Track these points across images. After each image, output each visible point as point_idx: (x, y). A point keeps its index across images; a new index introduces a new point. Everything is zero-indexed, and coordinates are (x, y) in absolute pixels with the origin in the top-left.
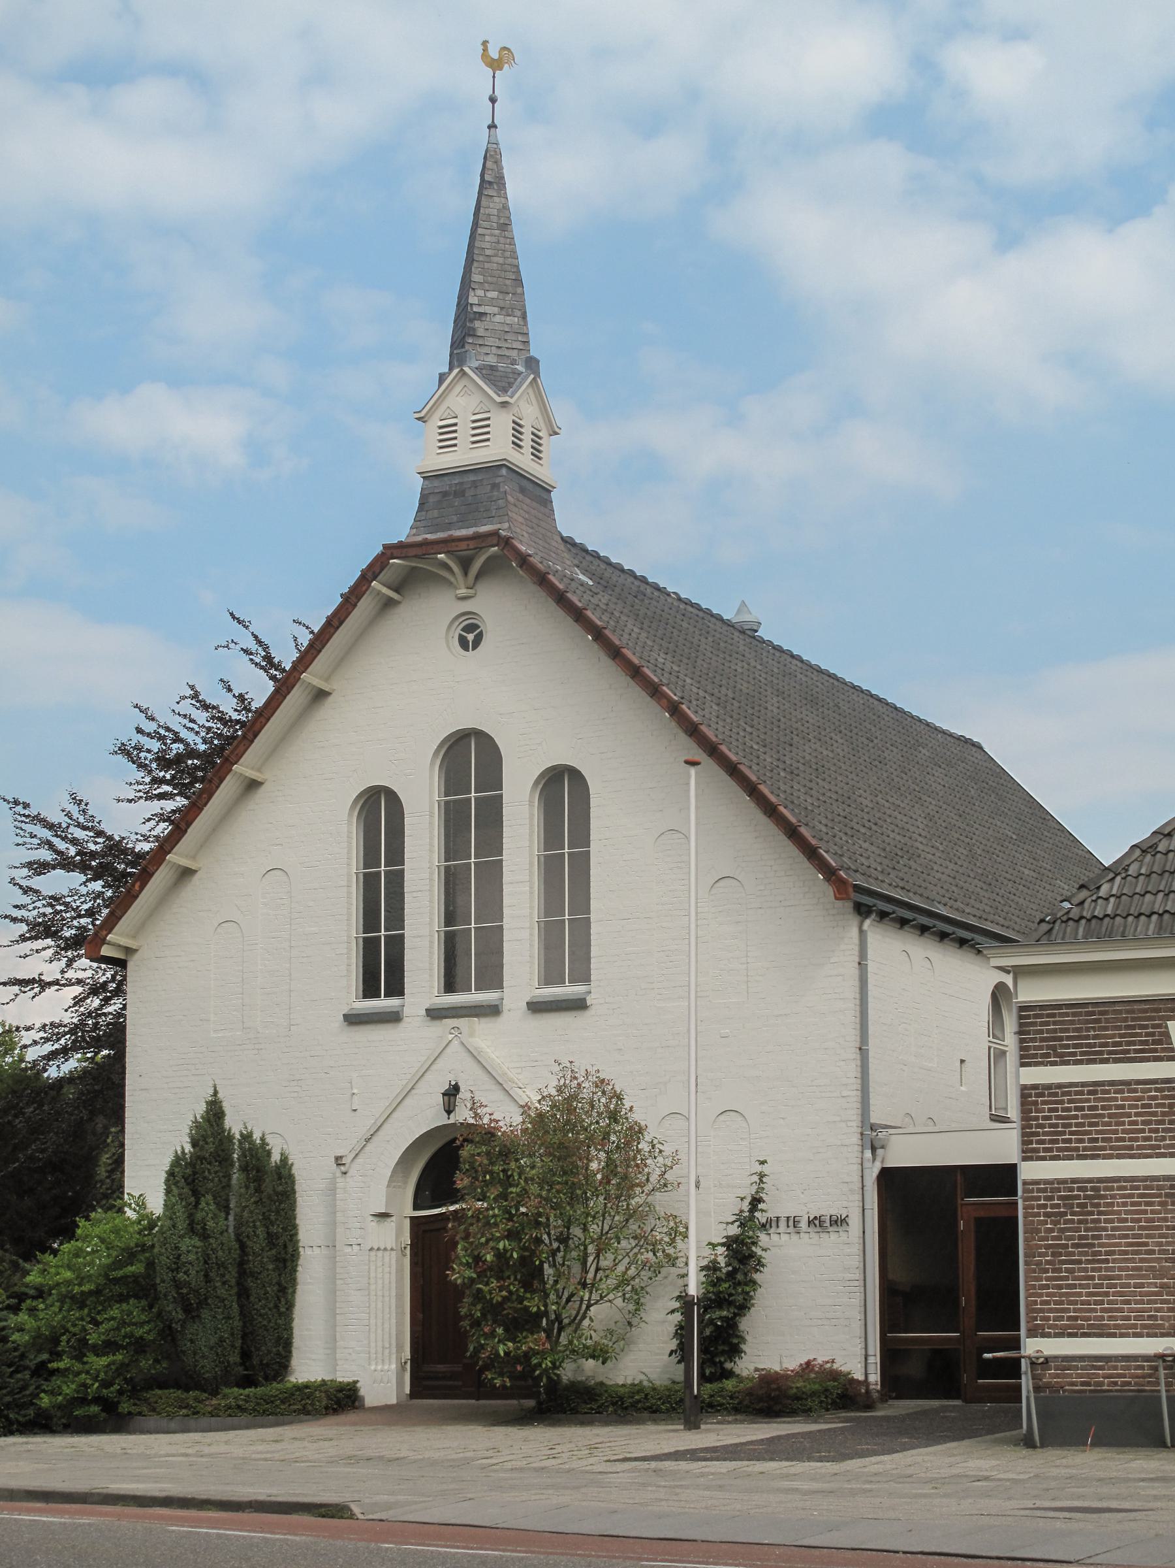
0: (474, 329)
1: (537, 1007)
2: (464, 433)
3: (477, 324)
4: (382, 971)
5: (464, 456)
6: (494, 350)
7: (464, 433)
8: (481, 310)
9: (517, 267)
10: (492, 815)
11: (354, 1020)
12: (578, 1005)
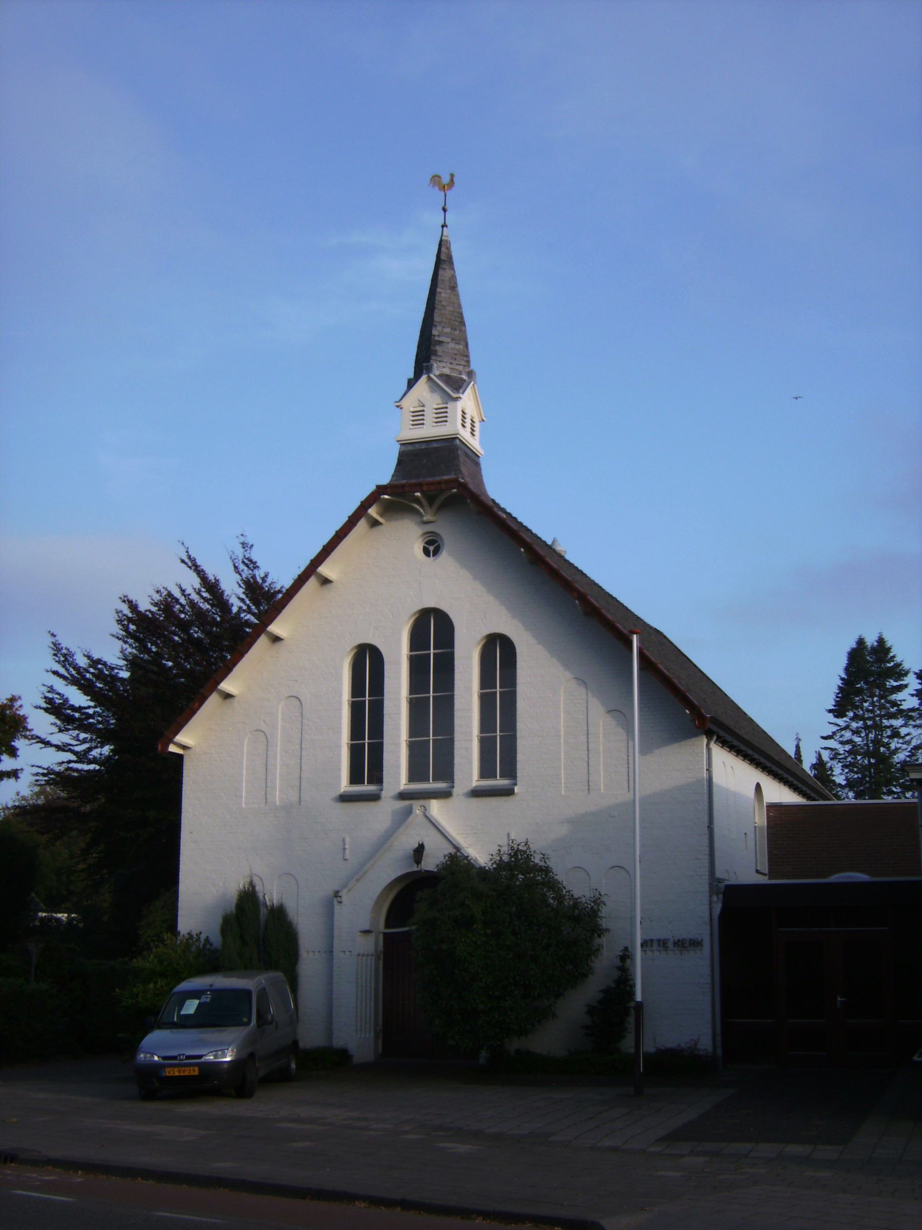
0: (436, 351)
1: (477, 793)
2: (430, 416)
3: (438, 348)
4: (367, 762)
5: (430, 430)
6: (448, 365)
7: (430, 416)
8: (441, 339)
9: (462, 314)
10: (446, 665)
11: (345, 798)
12: (508, 792)
